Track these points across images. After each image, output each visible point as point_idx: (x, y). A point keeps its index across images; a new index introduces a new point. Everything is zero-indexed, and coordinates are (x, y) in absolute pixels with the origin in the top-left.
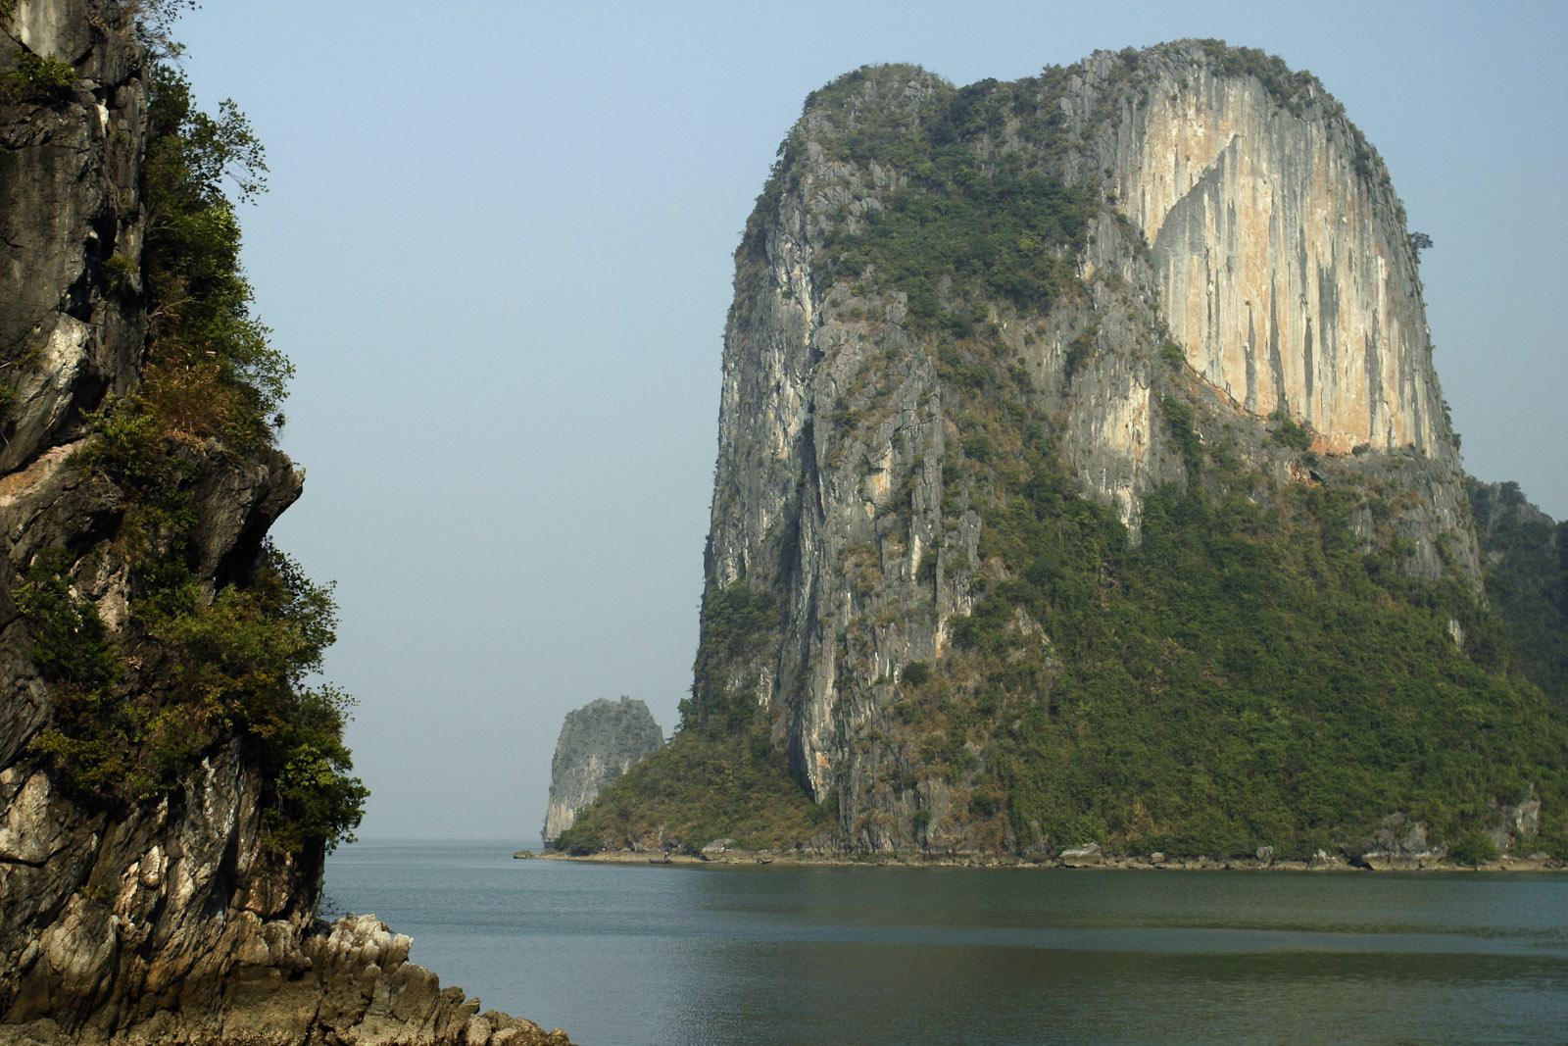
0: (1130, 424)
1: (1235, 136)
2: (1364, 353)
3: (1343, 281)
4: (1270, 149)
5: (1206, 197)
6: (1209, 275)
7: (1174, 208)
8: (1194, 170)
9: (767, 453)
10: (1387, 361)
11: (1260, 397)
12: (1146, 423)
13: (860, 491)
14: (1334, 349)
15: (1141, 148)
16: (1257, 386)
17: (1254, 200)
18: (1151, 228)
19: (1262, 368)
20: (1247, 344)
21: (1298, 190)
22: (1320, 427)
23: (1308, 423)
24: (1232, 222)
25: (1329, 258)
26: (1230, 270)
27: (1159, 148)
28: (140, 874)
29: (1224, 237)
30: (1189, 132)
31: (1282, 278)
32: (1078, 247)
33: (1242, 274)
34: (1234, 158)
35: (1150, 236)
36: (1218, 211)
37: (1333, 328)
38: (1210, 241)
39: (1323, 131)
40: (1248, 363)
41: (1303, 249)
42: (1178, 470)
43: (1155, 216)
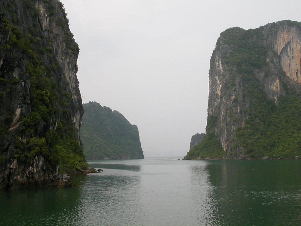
1: (293, 36)
5: (288, 46)
8: (286, 42)
9: (216, 93)
12: (279, 85)
13: (230, 99)
15: (277, 39)
16: (298, 78)
17: (297, 46)
18: (279, 52)
24: (293, 50)
26: (293, 59)
27: (279, 39)
28: (29, 170)
29: (292, 53)
34: (293, 40)
35: (279, 54)
36: (290, 49)
38: (289, 54)
40: (297, 74)
42: (284, 93)
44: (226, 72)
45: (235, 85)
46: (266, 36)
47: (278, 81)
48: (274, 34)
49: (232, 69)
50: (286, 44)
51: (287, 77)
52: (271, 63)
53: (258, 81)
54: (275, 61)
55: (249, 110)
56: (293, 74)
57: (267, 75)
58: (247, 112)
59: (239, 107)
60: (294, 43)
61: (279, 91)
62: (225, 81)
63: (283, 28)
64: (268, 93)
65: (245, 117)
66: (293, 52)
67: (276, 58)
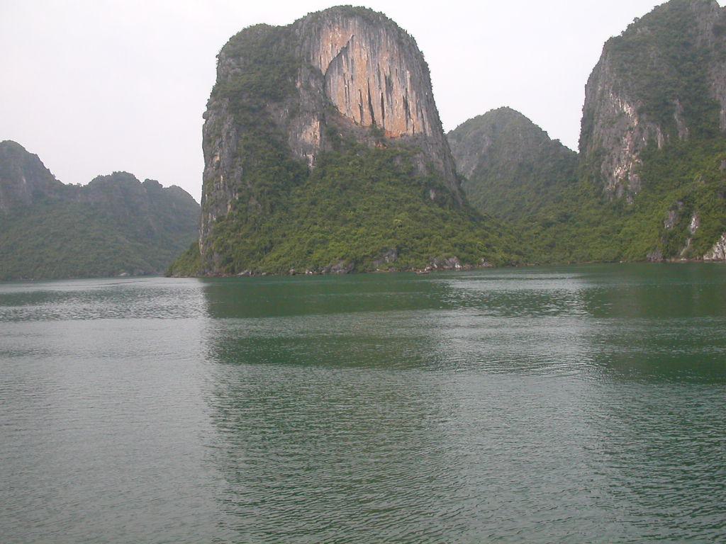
3: (394, 80)
8: (339, 48)
10: (411, 105)
11: (365, 120)
15: (319, 43)
19: (366, 110)
22: (388, 128)
23: (384, 128)
24: (352, 64)
25: (388, 73)
27: (325, 43)
32: (295, 78)
33: (357, 80)
36: (348, 61)
42: (329, 148)
44: (210, 111)
45: (220, 136)
46: (301, 38)
47: (316, 124)
49: (220, 105)
50: (339, 52)
51: (340, 117)
53: (273, 125)
54: (313, 85)
55: (239, 181)
56: (352, 110)
57: (292, 115)
63: (334, 21)
66: (353, 68)
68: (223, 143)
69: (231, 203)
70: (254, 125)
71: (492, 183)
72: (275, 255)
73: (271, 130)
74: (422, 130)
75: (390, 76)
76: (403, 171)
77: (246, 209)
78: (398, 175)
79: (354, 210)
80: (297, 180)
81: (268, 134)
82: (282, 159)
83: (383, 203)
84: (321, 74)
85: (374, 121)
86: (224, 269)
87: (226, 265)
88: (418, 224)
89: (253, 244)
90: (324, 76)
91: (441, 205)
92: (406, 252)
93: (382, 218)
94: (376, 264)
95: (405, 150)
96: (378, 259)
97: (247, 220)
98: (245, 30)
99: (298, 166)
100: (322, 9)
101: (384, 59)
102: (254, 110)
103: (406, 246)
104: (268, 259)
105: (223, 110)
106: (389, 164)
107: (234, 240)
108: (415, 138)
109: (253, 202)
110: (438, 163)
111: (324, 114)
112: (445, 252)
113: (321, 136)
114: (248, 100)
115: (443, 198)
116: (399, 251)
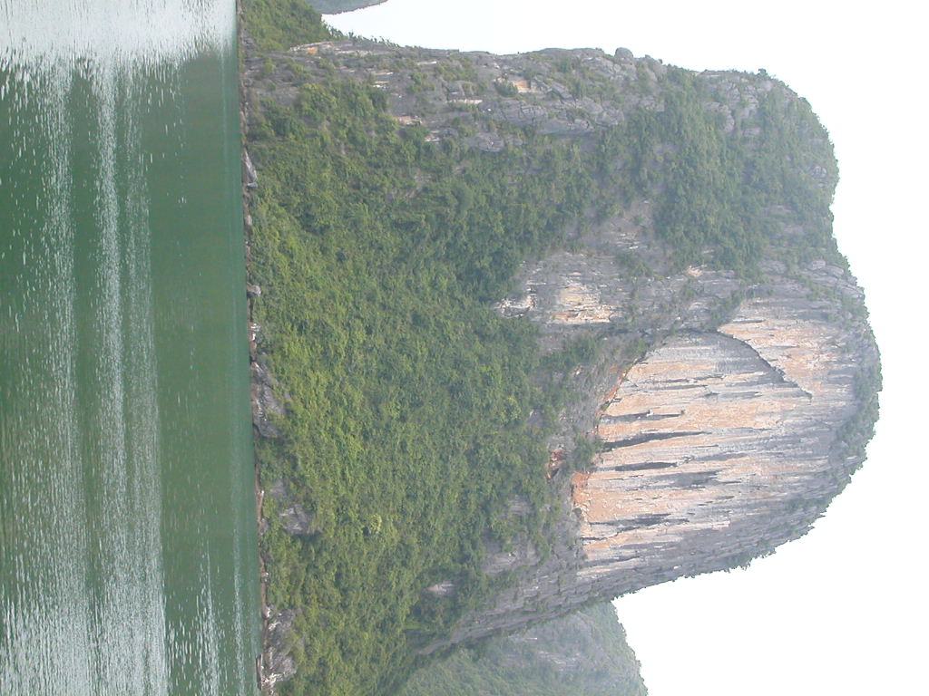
0: (581, 307)
1: (810, 396)
2: (654, 513)
3: (708, 492)
4: (805, 426)
5: (762, 373)
6: (700, 379)
7: (749, 347)
8: (780, 363)
10: (649, 534)
11: (612, 427)
13: (513, 74)
14: (655, 488)
15: (793, 318)
16: (620, 424)
17: (763, 414)
19: (635, 428)
20: (651, 414)
21: (774, 451)
22: (594, 479)
23: (596, 470)
24: (744, 396)
25: (724, 479)
26: (708, 396)
27: (794, 332)
30: (809, 356)
31: (704, 439)
32: (712, 265)
33: (705, 407)
35: (723, 329)
36: (751, 384)
37: (671, 486)
39: (822, 469)
40: (637, 416)
41: (729, 457)
42: (548, 346)
43: (743, 332)
44: (633, 67)
45: (576, 94)
46: (805, 273)
47: (603, 315)
48: (817, 304)
49: (647, 91)
50: (772, 364)
51: (620, 369)
52: (685, 286)
53: (601, 217)
54: (694, 306)
55: (467, 144)
56: (636, 396)
57: (625, 261)
58: (457, 135)
59: (477, 102)
60: (776, 403)
61: (556, 321)
62: (594, 62)
63: (844, 350)
64: (545, 266)
65: (433, 129)
66: (736, 396)
67: (707, 311)
68: (558, 103)
69: (417, 124)
70: (602, 171)
71: (469, 680)
72: (293, 242)
73: (589, 212)
74: (591, 557)
75: (717, 483)
76: (494, 520)
77: (403, 164)
78: (485, 507)
79: (403, 419)
80: (472, 276)
81: (579, 206)
82: (520, 240)
83: (419, 484)
84: (720, 324)
85: (610, 446)
86: (258, 113)
87: (268, 117)
88: (372, 571)
89: (321, 186)
90: (714, 331)
91: (416, 611)
92: (304, 554)
93: (383, 486)
94: (276, 488)
95: (544, 521)
96: (288, 491)
97: (377, 166)
98: (825, 135)
99: (503, 277)
100: (873, 321)
101: (753, 468)
102: (635, 171)
103: (319, 552)
104: (286, 225)
105: (634, 99)
106: (511, 488)
107: (328, 139)
108: (572, 544)
109: (419, 180)
110: (515, 598)
111: (625, 331)
112: (307, 646)
113: (576, 327)
114: (660, 158)
115: (433, 614)
116: (308, 539)
